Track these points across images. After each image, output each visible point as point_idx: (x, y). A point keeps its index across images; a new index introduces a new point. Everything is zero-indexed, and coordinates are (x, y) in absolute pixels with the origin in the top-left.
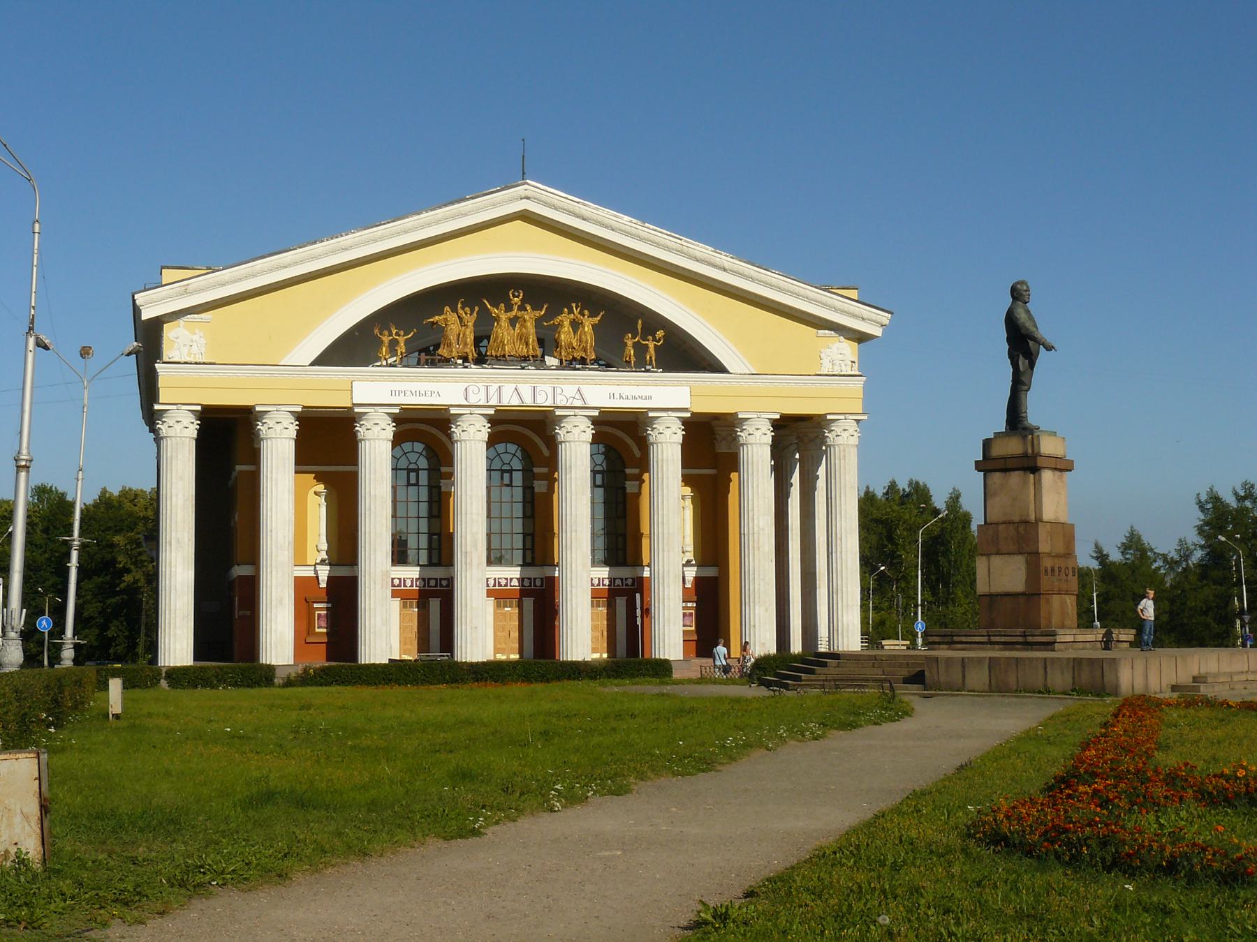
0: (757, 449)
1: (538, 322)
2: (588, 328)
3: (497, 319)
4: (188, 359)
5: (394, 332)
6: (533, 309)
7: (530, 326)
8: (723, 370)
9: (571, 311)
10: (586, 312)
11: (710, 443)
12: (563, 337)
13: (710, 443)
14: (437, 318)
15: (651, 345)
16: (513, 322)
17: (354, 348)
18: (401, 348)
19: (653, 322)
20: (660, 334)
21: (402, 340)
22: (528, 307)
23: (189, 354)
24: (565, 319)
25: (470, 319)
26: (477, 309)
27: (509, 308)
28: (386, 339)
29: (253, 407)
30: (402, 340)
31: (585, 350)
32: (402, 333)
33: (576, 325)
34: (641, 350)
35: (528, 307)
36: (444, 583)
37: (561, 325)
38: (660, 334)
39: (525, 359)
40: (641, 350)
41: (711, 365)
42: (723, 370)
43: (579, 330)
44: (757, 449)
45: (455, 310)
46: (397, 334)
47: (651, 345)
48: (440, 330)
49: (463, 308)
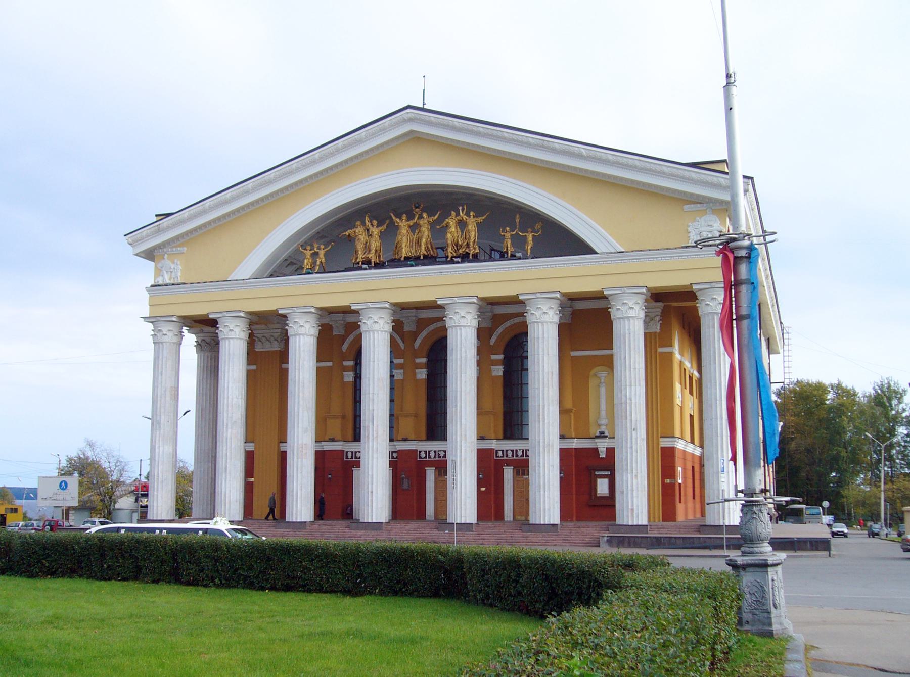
0: (631, 325)
1: (432, 225)
2: (472, 227)
3: (398, 228)
4: (168, 282)
5: (316, 246)
6: (429, 216)
7: (425, 232)
8: (593, 252)
9: (458, 214)
10: (472, 213)
11: (588, 322)
12: (449, 236)
13: (588, 322)
14: (349, 231)
15: (530, 238)
16: (414, 228)
17: (288, 264)
18: (322, 257)
19: (531, 218)
20: (538, 226)
21: (322, 253)
22: (425, 215)
23: (171, 278)
24: (452, 222)
25: (375, 231)
26: (387, 222)
27: (410, 218)
28: (308, 253)
29: (208, 315)
30: (322, 253)
31: (468, 245)
32: (322, 247)
33: (462, 224)
34: (519, 242)
35: (425, 215)
36: (442, 454)
37: (447, 226)
38: (538, 226)
39: (418, 258)
40: (519, 242)
41: (579, 247)
42: (596, 253)
43: (463, 229)
44: (631, 325)
45: (363, 224)
46: (319, 249)
47: (530, 238)
48: (351, 239)
49: (371, 221)
